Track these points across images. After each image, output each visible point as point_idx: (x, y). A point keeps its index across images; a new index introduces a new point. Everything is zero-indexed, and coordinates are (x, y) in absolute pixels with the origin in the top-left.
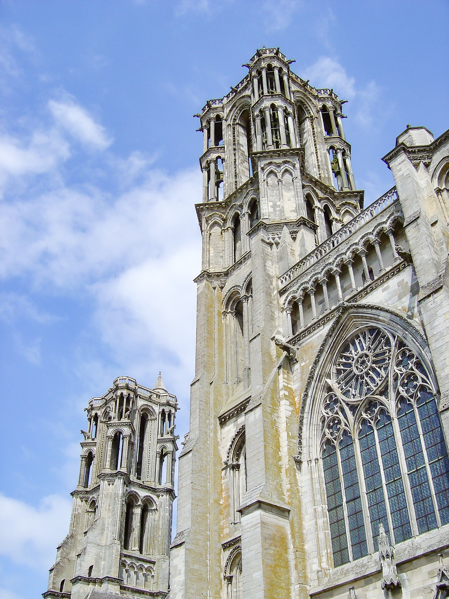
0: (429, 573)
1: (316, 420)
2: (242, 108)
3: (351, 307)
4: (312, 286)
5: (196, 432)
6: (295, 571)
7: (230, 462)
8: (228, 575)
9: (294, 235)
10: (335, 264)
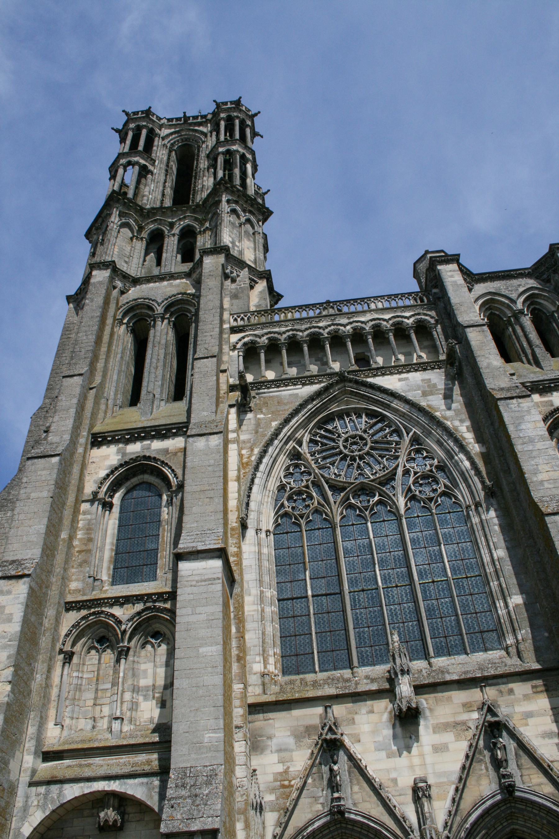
0: (464, 705)
1: (273, 484)
2: (186, 140)
3: (350, 381)
4: (285, 339)
5: (64, 436)
6: (236, 664)
7: (101, 495)
8: (67, 648)
9: (253, 283)
10: (327, 331)
